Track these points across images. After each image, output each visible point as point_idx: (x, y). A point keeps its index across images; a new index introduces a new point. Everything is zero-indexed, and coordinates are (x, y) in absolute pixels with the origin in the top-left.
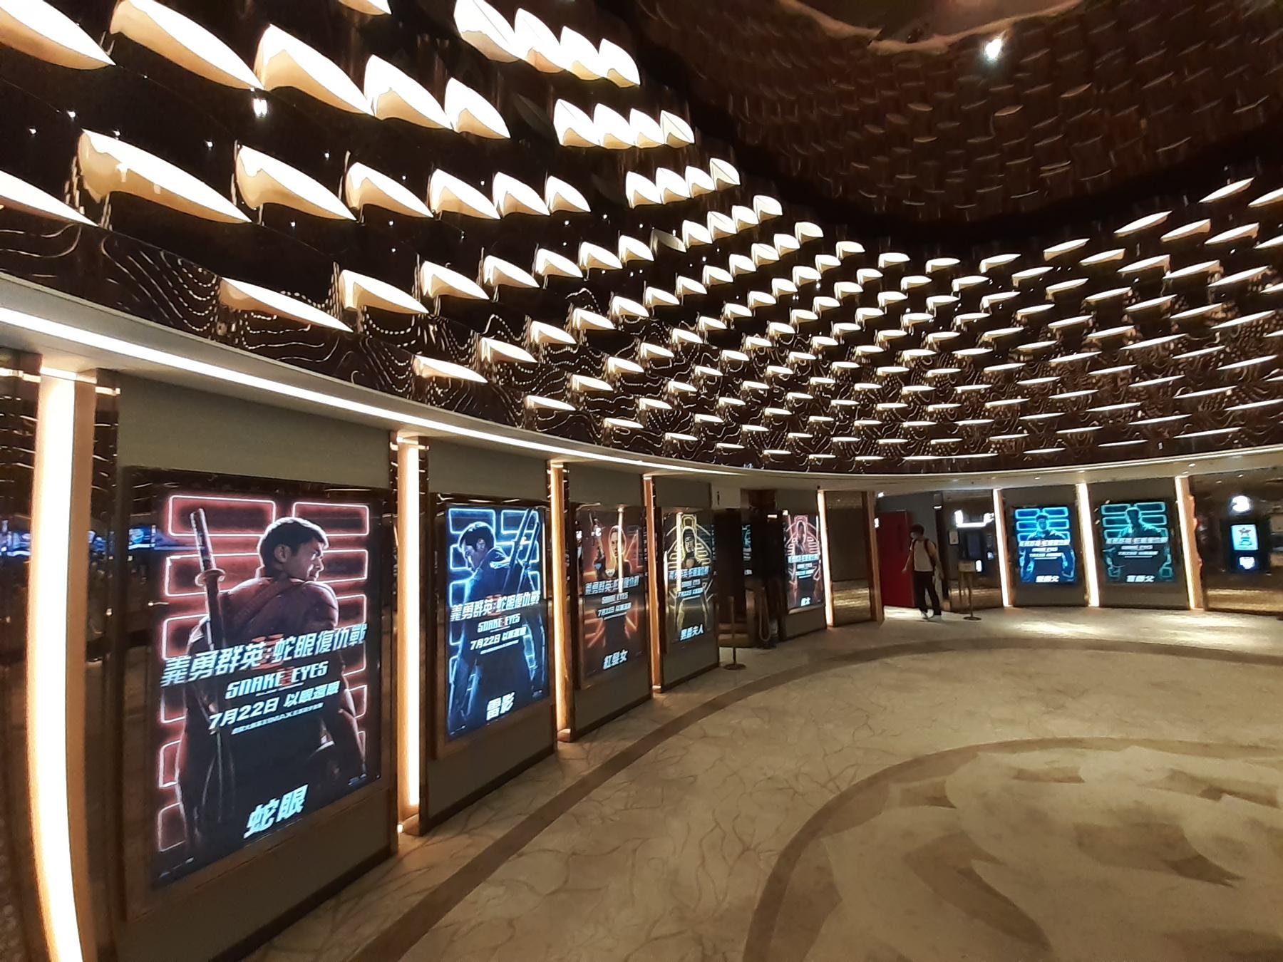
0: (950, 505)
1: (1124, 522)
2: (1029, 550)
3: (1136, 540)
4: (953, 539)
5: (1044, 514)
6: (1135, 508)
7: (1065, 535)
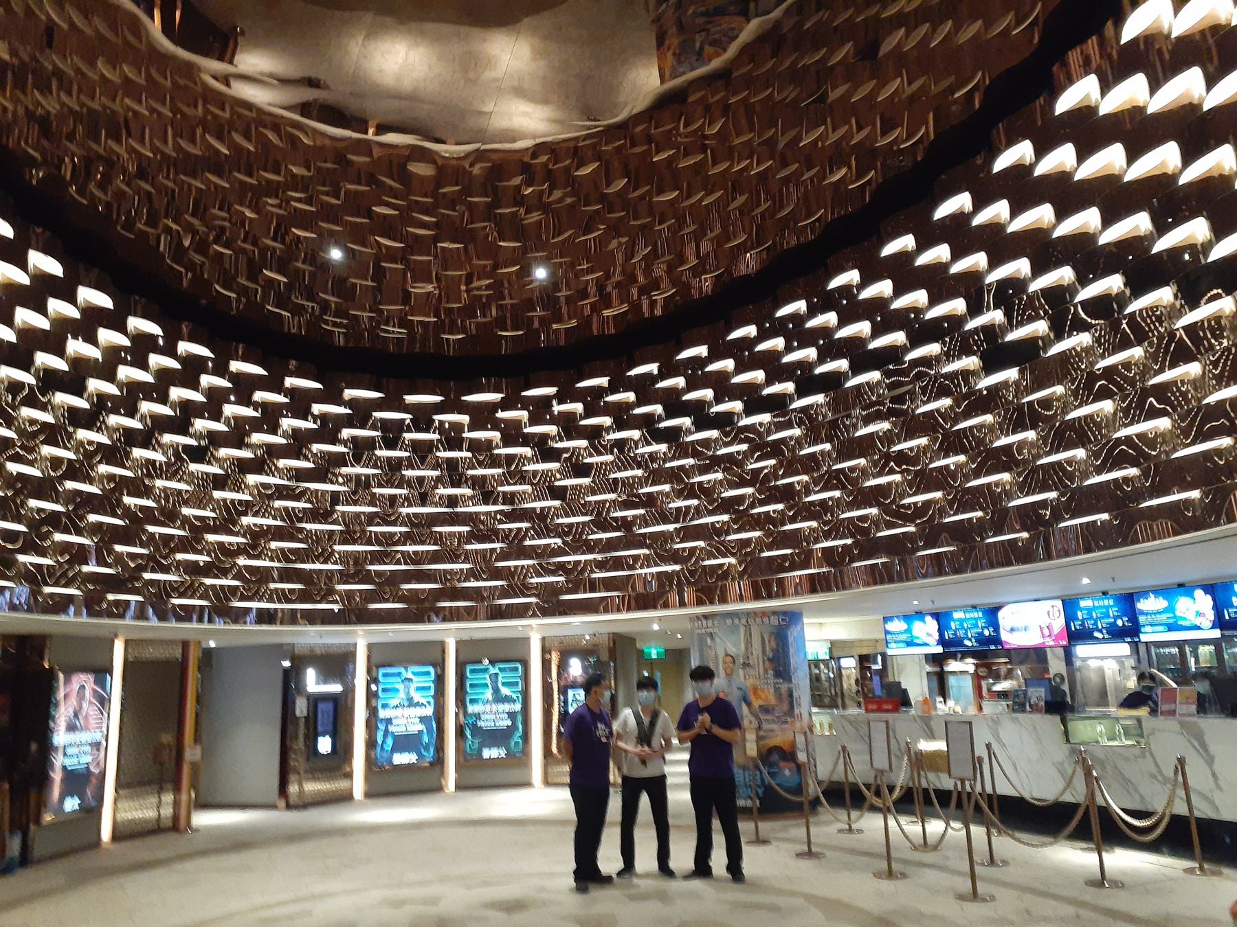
0: (300, 661)
1: (486, 685)
2: (389, 721)
3: (494, 707)
4: (301, 707)
5: (410, 675)
6: (497, 671)
7: (429, 703)
